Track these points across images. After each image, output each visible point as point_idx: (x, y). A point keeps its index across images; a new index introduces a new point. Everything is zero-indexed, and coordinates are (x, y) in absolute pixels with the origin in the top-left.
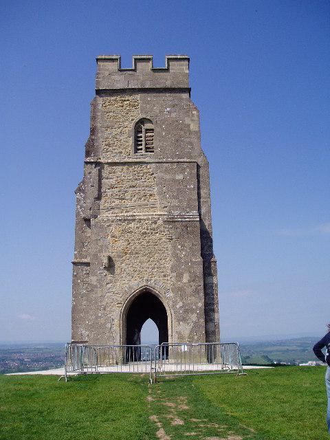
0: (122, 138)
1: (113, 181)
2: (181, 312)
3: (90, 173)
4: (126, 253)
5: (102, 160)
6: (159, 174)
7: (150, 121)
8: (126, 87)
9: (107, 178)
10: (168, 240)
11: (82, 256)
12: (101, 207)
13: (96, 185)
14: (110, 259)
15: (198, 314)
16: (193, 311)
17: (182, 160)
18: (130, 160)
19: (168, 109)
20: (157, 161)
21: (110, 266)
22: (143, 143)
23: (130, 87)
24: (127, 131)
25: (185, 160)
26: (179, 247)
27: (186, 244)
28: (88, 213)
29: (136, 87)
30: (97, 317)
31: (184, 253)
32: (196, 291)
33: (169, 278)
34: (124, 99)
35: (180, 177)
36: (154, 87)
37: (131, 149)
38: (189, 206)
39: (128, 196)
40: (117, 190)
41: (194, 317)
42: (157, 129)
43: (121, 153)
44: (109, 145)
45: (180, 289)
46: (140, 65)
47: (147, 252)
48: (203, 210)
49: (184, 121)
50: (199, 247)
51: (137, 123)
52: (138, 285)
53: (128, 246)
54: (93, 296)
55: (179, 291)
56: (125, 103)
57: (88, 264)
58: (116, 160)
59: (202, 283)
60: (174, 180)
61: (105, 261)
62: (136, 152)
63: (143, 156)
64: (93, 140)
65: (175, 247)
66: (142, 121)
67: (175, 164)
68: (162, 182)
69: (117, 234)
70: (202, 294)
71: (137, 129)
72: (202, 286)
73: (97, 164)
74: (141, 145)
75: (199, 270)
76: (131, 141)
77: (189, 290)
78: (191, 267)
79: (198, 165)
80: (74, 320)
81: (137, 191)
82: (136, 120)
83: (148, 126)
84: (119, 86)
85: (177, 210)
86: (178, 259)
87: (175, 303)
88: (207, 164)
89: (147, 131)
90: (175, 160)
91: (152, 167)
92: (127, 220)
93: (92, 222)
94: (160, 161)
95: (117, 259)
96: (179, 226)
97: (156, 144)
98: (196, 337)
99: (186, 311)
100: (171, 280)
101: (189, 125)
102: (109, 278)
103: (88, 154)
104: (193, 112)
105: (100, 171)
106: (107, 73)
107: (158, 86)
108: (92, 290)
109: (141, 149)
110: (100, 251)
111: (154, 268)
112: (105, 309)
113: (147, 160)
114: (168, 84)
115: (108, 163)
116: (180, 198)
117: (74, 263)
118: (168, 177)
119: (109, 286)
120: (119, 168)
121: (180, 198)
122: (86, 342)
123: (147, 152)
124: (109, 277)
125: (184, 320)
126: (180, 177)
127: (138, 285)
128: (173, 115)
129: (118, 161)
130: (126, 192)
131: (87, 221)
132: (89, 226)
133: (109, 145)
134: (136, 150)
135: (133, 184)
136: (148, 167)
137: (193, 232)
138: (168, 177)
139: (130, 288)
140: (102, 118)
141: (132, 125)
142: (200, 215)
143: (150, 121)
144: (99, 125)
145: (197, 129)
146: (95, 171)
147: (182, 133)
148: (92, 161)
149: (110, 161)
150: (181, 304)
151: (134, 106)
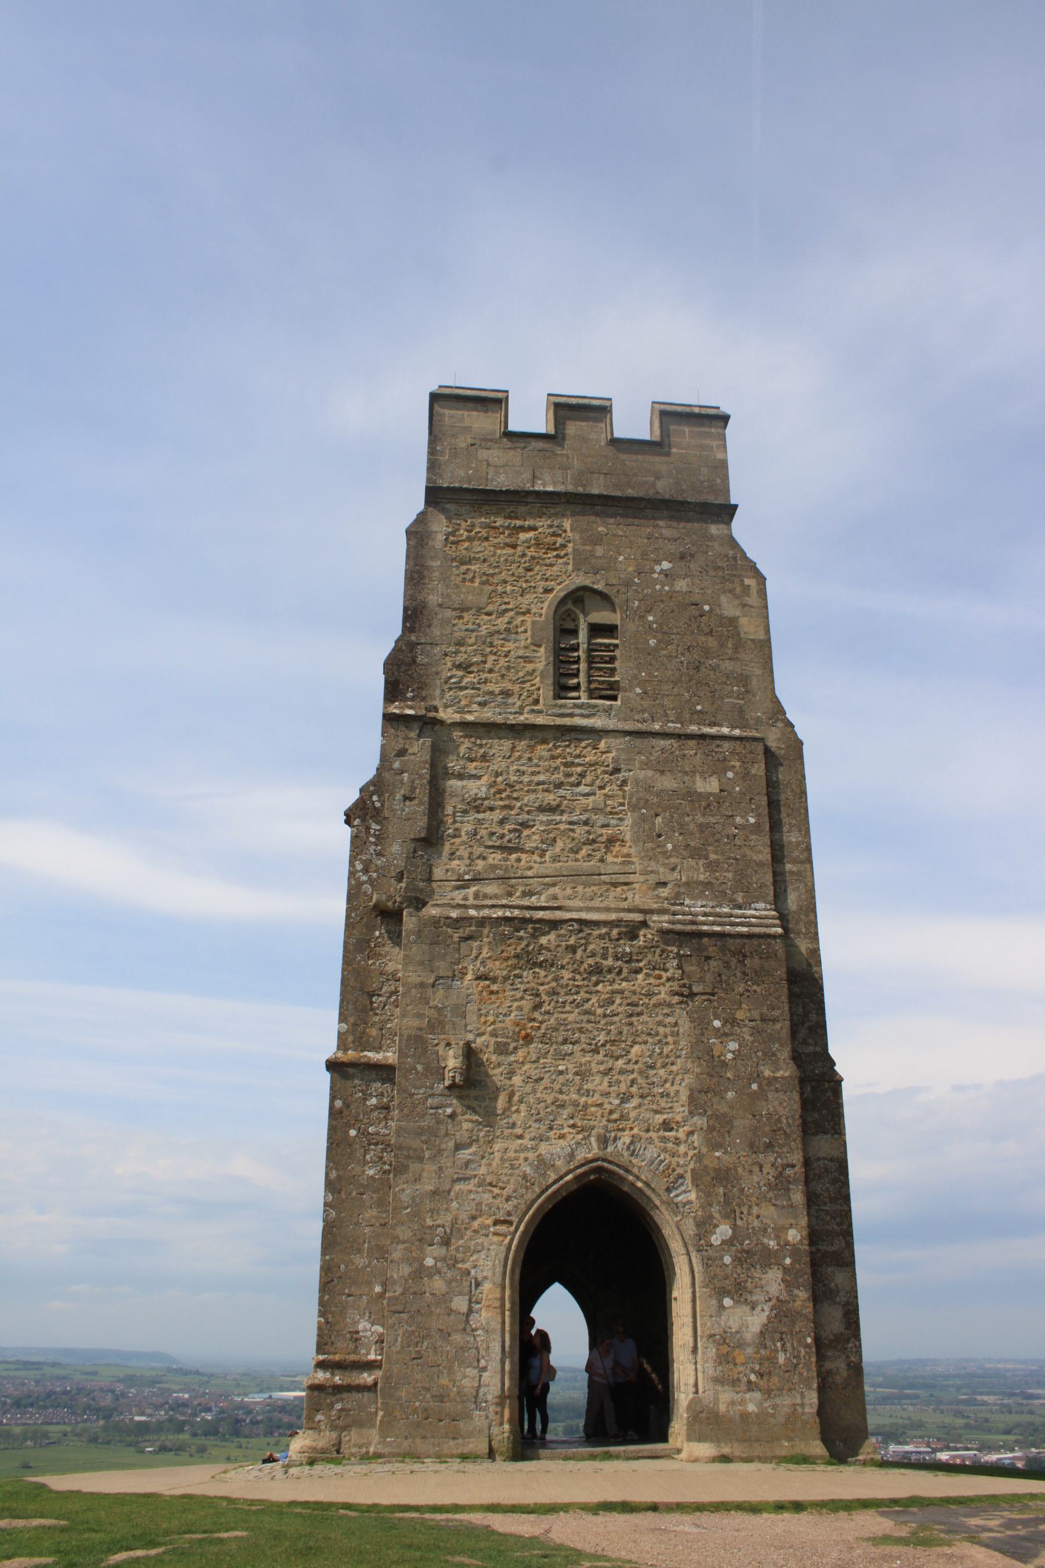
0: (510, 646)
1: (477, 788)
2: (727, 1260)
3: (402, 753)
4: (528, 1039)
5: (442, 715)
6: (636, 773)
7: (604, 598)
8: (528, 487)
9: (460, 776)
10: (676, 999)
11: (363, 1044)
12: (438, 873)
13: (423, 794)
14: (470, 1053)
15: (786, 1270)
16: (768, 1259)
17: (713, 731)
18: (540, 720)
19: (666, 565)
20: (629, 726)
21: (473, 1084)
22: (583, 666)
23: (539, 487)
24: (529, 625)
25: (725, 730)
26: (717, 1023)
27: (740, 1015)
28: (396, 890)
29: (560, 488)
30: (420, 1273)
31: (733, 1046)
32: (780, 1184)
33: (681, 1134)
34: (518, 523)
35: (712, 785)
36: (619, 494)
37: (546, 693)
38: (742, 883)
39: (532, 839)
40: (497, 815)
41: (773, 1281)
42: (629, 628)
43: (507, 694)
44: (465, 667)
45: (724, 1176)
46: (572, 428)
47: (602, 1038)
48: (792, 901)
49: (715, 604)
50: (782, 1027)
51: (562, 602)
52: (572, 1155)
53: (536, 1015)
54: (405, 1191)
55: (716, 1180)
56: (523, 536)
57: (385, 1072)
58: (488, 714)
59: (797, 1158)
60: (692, 796)
61: (453, 1061)
62: (557, 696)
63: (582, 711)
64: (412, 646)
65: (701, 1024)
66: (578, 597)
67: (692, 743)
68: (648, 804)
69: (497, 968)
70: (798, 1197)
71: (564, 628)
72: (799, 1169)
73: (427, 723)
74: (576, 675)
75: (785, 1106)
76: (543, 658)
77: (753, 1181)
78: (754, 1096)
79: (767, 751)
80: (331, 1281)
81: (562, 827)
82: (560, 591)
83: (602, 616)
84: (501, 481)
85: (701, 895)
86: (714, 1066)
87: (705, 1226)
88: (797, 746)
89: (596, 630)
90: (693, 728)
91: (611, 750)
92: (531, 920)
93: (409, 921)
94: (643, 727)
95: (494, 1058)
96: (712, 951)
97: (623, 670)
98: (781, 1358)
99: (745, 1258)
100: (689, 1144)
101: (733, 621)
102: (466, 1126)
103: (393, 690)
104: (747, 582)
105: (438, 753)
106: (462, 442)
107: (630, 492)
108: (400, 1169)
109: (577, 688)
110: (436, 1025)
111: (625, 1098)
112: (446, 1242)
113: (597, 722)
114: (664, 487)
115: (464, 725)
116: (713, 857)
117: (332, 1066)
118: (667, 783)
119: (465, 1154)
120: (500, 747)
121: (713, 857)
122: (370, 1366)
123: (591, 697)
124: (467, 1123)
125: (739, 1291)
126: (712, 785)
127: (572, 1155)
128: (681, 585)
129: (499, 719)
130: (525, 825)
131: (390, 916)
132: (396, 938)
133: (465, 667)
134: (562, 690)
135: (551, 798)
136: (602, 745)
137: (759, 975)
138: (667, 783)
139: (542, 1164)
140: (445, 579)
141: (544, 608)
142: (783, 918)
143: (604, 598)
144: (433, 599)
145: (762, 637)
146: (419, 748)
147: (712, 643)
148: (411, 712)
149: (470, 718)
150: (723, 1231)
151: (552, 547)
